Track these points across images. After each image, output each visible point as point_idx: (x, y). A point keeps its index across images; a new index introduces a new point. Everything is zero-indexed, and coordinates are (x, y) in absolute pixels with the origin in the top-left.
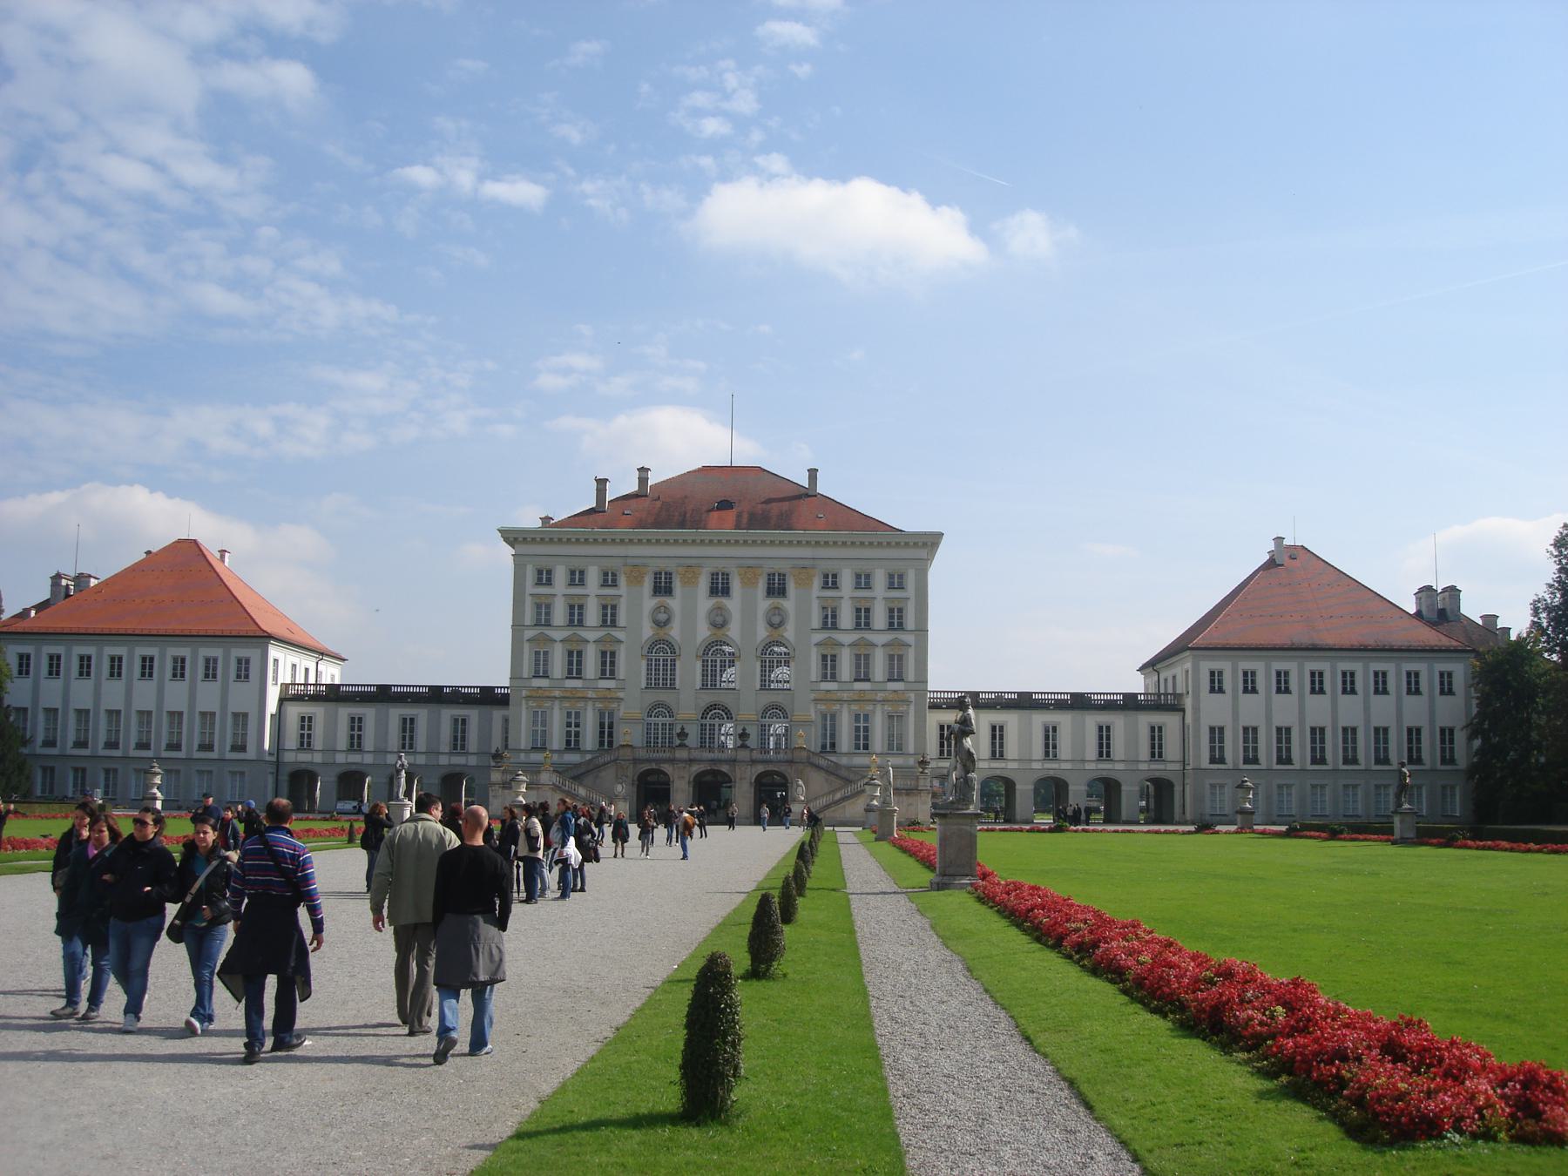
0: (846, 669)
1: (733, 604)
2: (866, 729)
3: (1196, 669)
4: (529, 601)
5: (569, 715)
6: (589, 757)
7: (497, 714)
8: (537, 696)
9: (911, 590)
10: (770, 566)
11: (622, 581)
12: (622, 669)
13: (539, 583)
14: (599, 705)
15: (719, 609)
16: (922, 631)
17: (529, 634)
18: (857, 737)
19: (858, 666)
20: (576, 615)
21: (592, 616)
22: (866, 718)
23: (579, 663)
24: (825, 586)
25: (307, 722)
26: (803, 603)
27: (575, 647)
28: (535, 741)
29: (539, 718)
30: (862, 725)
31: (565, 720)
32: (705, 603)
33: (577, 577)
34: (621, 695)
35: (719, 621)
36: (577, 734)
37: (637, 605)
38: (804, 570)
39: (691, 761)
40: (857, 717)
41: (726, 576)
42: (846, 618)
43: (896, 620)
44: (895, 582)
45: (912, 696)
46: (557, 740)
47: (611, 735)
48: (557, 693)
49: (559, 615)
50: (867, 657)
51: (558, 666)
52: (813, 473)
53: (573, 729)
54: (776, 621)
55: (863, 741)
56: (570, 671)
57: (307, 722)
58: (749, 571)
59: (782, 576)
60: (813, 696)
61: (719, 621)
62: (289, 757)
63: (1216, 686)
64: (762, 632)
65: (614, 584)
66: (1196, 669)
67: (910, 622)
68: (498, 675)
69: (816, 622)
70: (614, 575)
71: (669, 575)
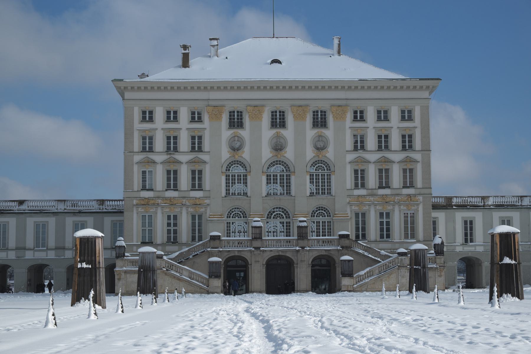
0: (372, 179)
1: (288, 133)
2: (388, 223)
5: (169, 217)
11: (206, 118)
13: (144, 119)
14: (191, 210)
16: (426, 150)
17: (137, 158)
18: (382, 230)
19: (381, 177)
20: (172, 144)
21: (184, 144)
22: (388, 215)
23: (175, 179)
27: (172, 168)
28: (144, 237)
30: (385, 220)
31: (166, 221)
32: (268, 134)
33: (172, 116)
34: (207, 201)
35: (278, 147)
36: (175, 232)
38: (340, 108)
40: (381, 215)
41: (282, 114)
42: (371, 143)
43: (407, 143)
46: (160, 236)
50: (387, 171)
53: (172, 228)
54: (320, 146)
61: (278, 147)
65: (200, 120)
68: (113, 191)
70: (199, 114)
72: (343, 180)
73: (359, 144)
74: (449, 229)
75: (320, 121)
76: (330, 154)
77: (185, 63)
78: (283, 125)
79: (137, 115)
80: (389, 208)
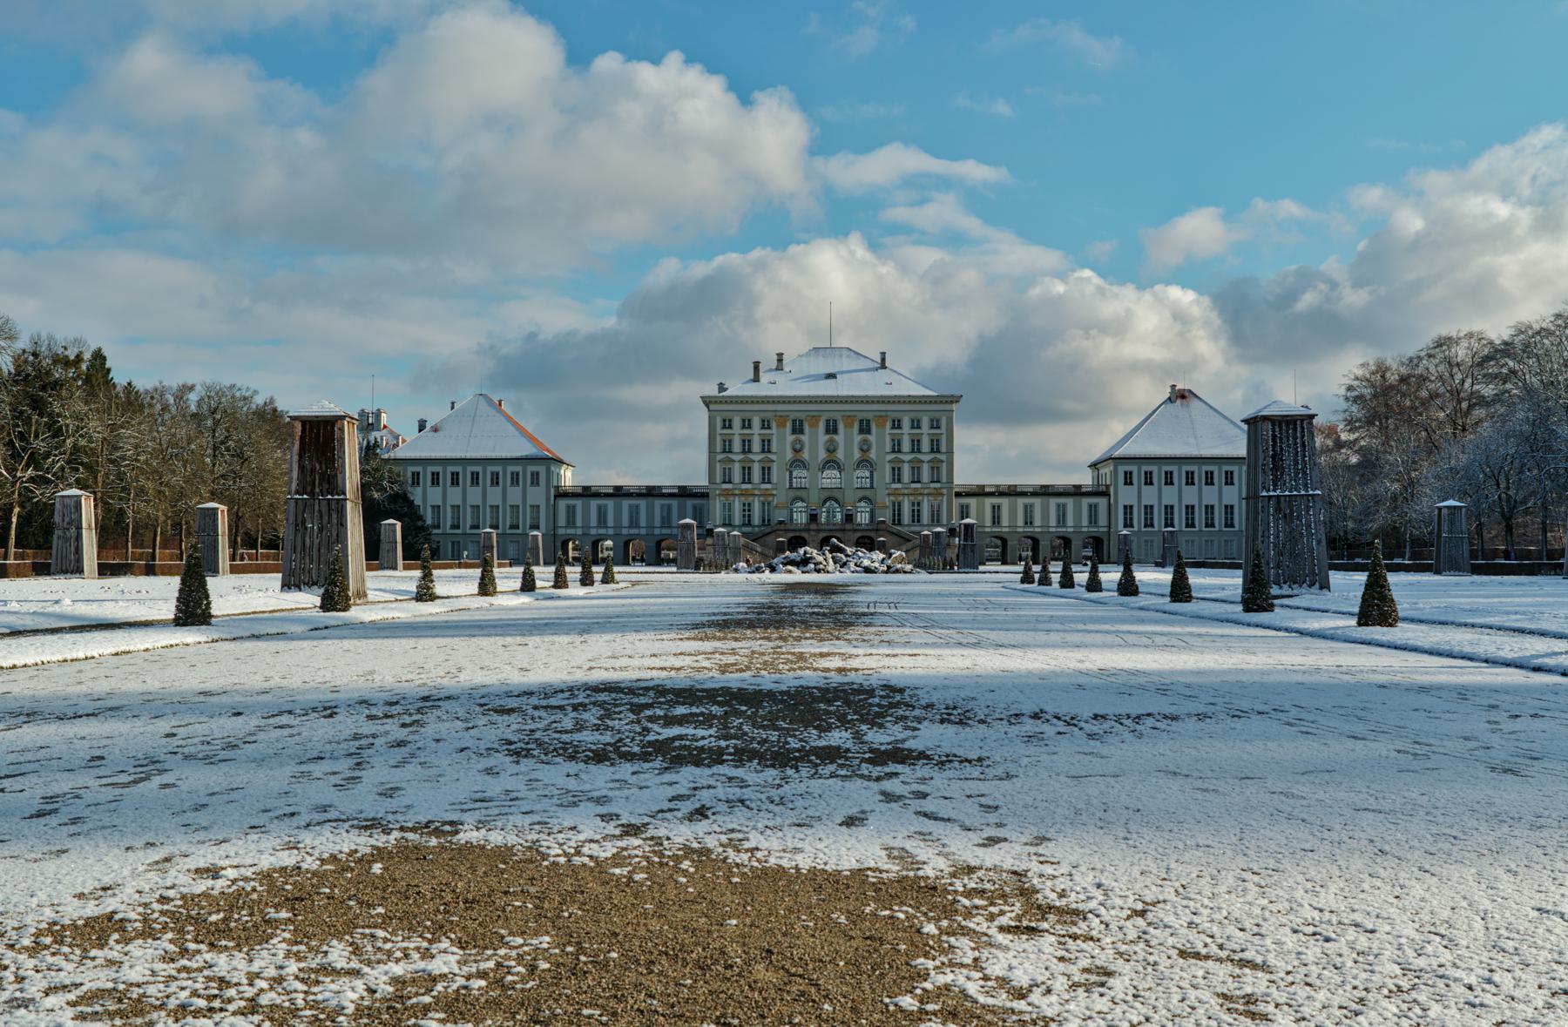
0: (906, 477)
1: (839, 439)
3: (1116, 470)
4: (719, 439)
8: (727, 493)
9: (943, 430)
10: (860, 416)
11: (774, 425)
12: (774, 480)
13: (724, 427)
15: (831, 441)
16: (950, 452)
17: (719, 457)
20: (747, 448)
24: (893, 427)
26: (881, 439)
32: (823, 438)
33: (747, 424)
37: (783, 440)
38: (881, 419)
39: (818, 531)
41: (835, 421)
43: (935, 449)
44: (935, 424)
49: (737, 447)
51: (737, 477)
52: (883, 354)
55: (916, 516)
57: (571, 511)
58: (849, 420)
66: (1116, 470)
67: (943, 448)
69: (888, 449)
71: (801, 422)
73: (897, 449)
74: (978, 514)
75: (865, 428)
76: (873, 455)
77: (756, 379)
78: (835, 431)
79: (719, 424)
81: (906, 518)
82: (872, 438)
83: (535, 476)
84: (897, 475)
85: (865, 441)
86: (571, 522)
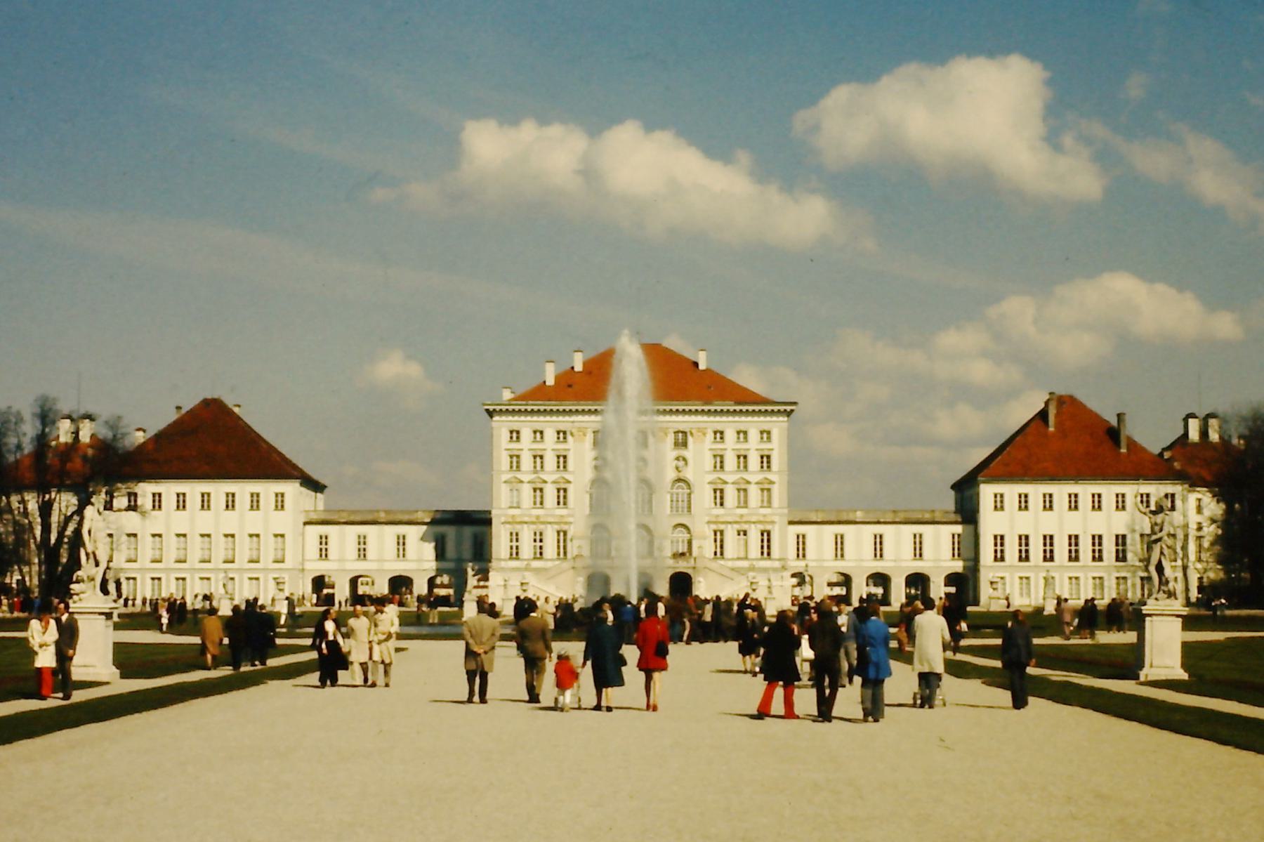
6: (549, 564)
7: (468, 531)
11: (569, 438)
17: (505, 477)
25: (324, 540)
26: (700, 452)
29: (515, 537)
34: (571, 519)
42: (730, 462)
44: (766, 434)
45: (776, 519)
47: (565, 548)
48: (526, 519)
53: (538, 544)
56: (535, 503)
57: (324, 540)
59: (684, 433)
60: (707, 519)
62: (308, 566)
63: (999, 505)
64: (671, 474)
72: (703, 498)
76: (689, 474)
80: (745, 527)
81: (730, 551)
82: (686, 453)
83: (280, 497)
84: (719, 497)
85: (684, 459)
86: (324, 554)
